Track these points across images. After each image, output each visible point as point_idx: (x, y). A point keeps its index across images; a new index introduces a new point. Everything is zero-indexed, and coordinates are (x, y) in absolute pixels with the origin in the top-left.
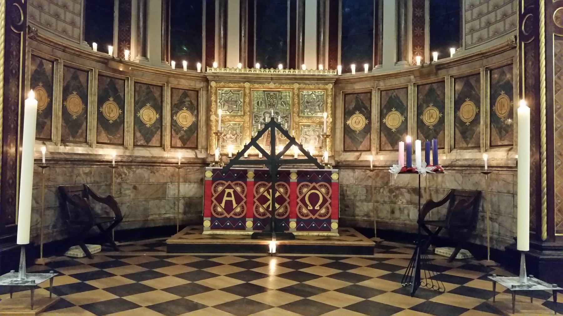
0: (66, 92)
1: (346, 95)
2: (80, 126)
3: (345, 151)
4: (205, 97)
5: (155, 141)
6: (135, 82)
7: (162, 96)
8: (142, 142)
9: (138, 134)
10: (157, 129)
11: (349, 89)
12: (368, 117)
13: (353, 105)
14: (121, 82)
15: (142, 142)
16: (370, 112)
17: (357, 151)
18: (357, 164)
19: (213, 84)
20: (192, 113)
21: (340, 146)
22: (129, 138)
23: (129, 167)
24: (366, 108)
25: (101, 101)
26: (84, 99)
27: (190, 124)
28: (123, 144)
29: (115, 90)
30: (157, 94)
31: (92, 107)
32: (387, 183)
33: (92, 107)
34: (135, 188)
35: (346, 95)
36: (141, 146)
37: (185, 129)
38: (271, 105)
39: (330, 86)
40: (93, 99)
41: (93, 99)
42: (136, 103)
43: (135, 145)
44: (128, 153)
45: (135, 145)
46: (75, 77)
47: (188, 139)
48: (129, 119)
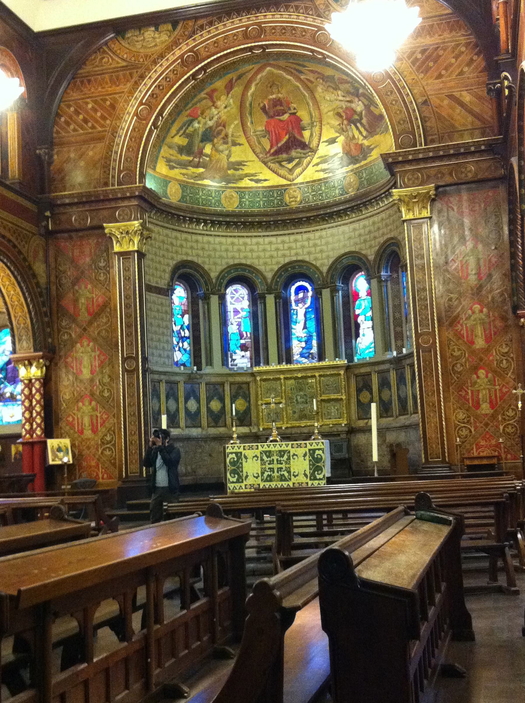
0: (167, 397)
1: (357, 376)
2: (176, 418)
3: (359, 419)
4: (254, 387)
5: (221, 422)
6: (206, 384)
7: (224, 391)
8: (213, 424)
9: (210, 419)
10: (222, 414)
11: (357, 371)
12: (371, 393)
13: (361, 385)
14: (197, 386)
15: (213, 424)
16: (372, 389)
17: (366, 419)
18: (366, 428)
19: (258, 378)
20: (246, 400)
21: (354, 416)
22: (204, 421)
23: (206, 442)
24: (370, 386)
25: (186, 400)
26: (177, 401)
27: (245, 408)
28: (200, 427)
29: (194, 391)
30: (221, 390)
31: (181, 406)
32: (385, 441)
33: (181, 406)
34: (210, 455)
35: (357, 376)
36: (213, 427)
37: (241, 412)
38: (301, 390)
39: (342, 372)
40: (181, 400)
41: (181, 400)
42: (207, 398)
43: (208, 427)
44: (204, 433)
45: (208, 427)
46: (171, 389)
47: (243, 420)
48: (204, 410)
